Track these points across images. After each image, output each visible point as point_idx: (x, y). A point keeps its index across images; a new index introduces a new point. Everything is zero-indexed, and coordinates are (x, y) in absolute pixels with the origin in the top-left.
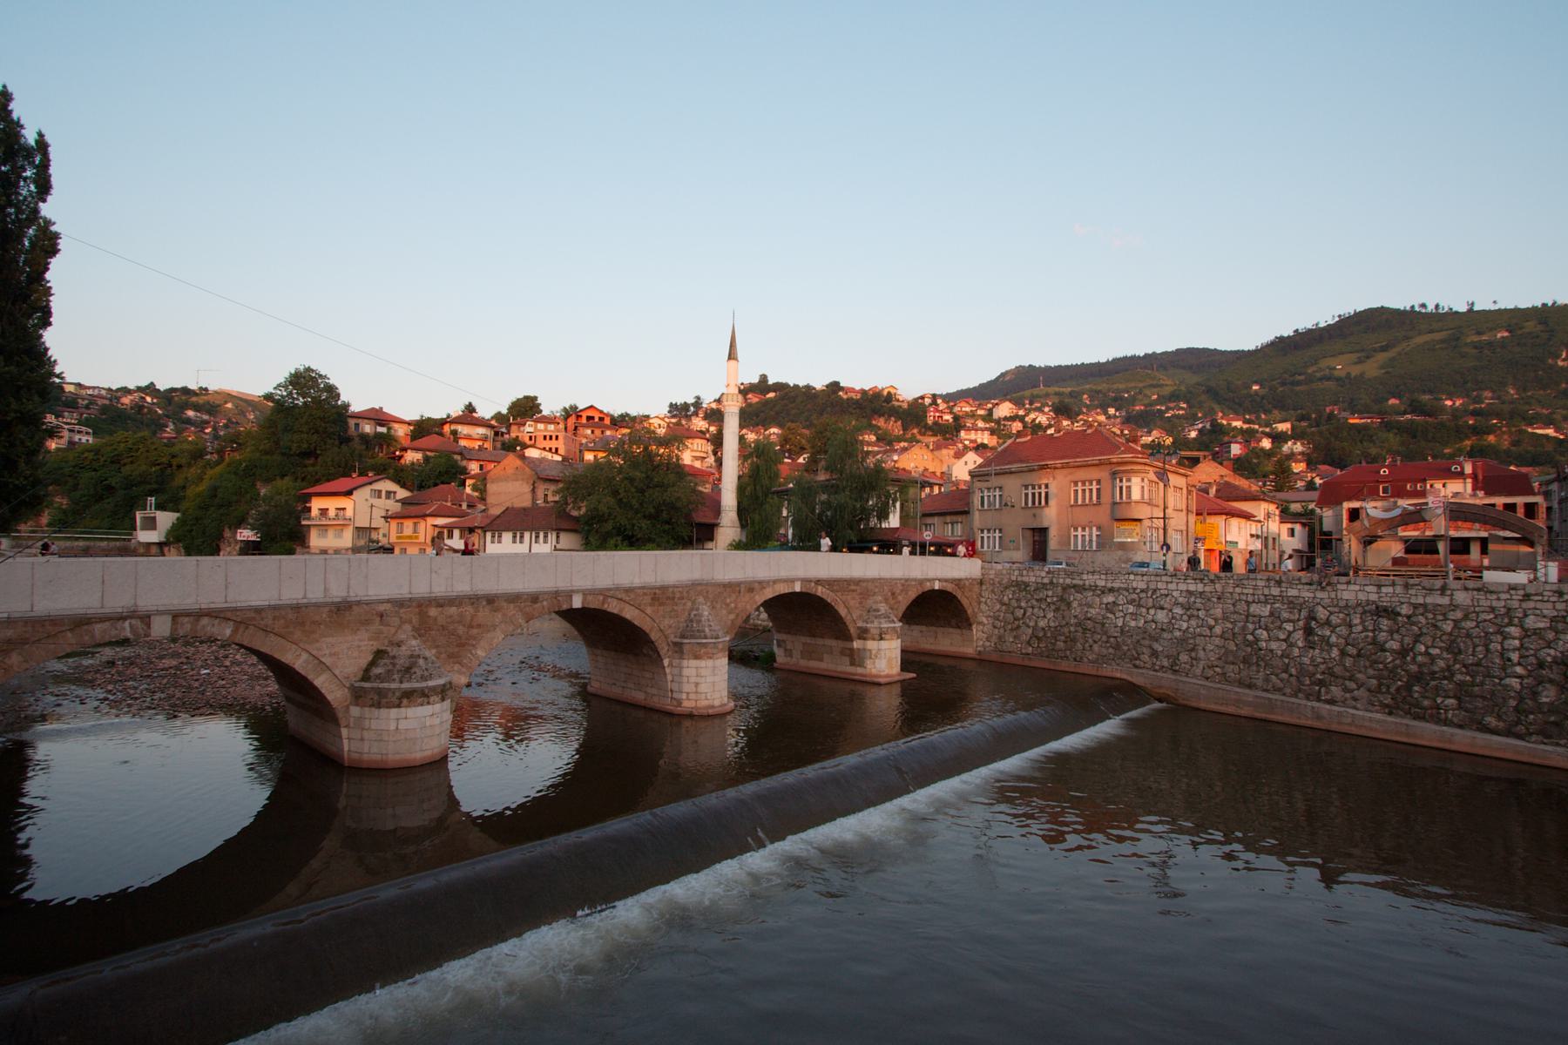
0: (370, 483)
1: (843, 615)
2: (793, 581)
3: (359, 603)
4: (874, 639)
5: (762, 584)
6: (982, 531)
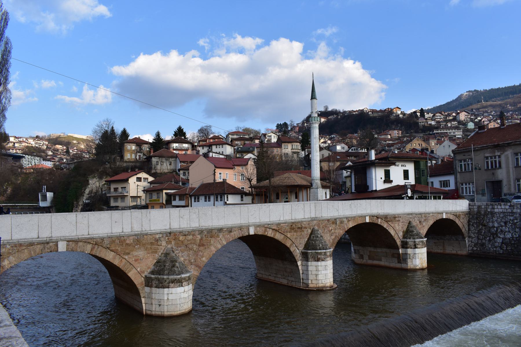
1: (393, 235)
4: (411, 248)
5: (348, 219)
6: (462, 185)
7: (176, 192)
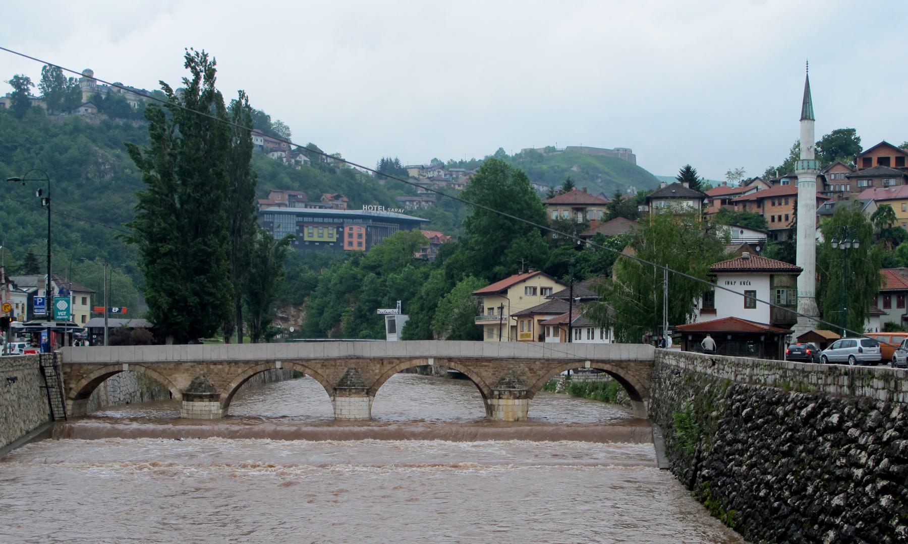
0: (524, 281)
2: (427, 358)
3: (184, 362)
7: (554, 320)
